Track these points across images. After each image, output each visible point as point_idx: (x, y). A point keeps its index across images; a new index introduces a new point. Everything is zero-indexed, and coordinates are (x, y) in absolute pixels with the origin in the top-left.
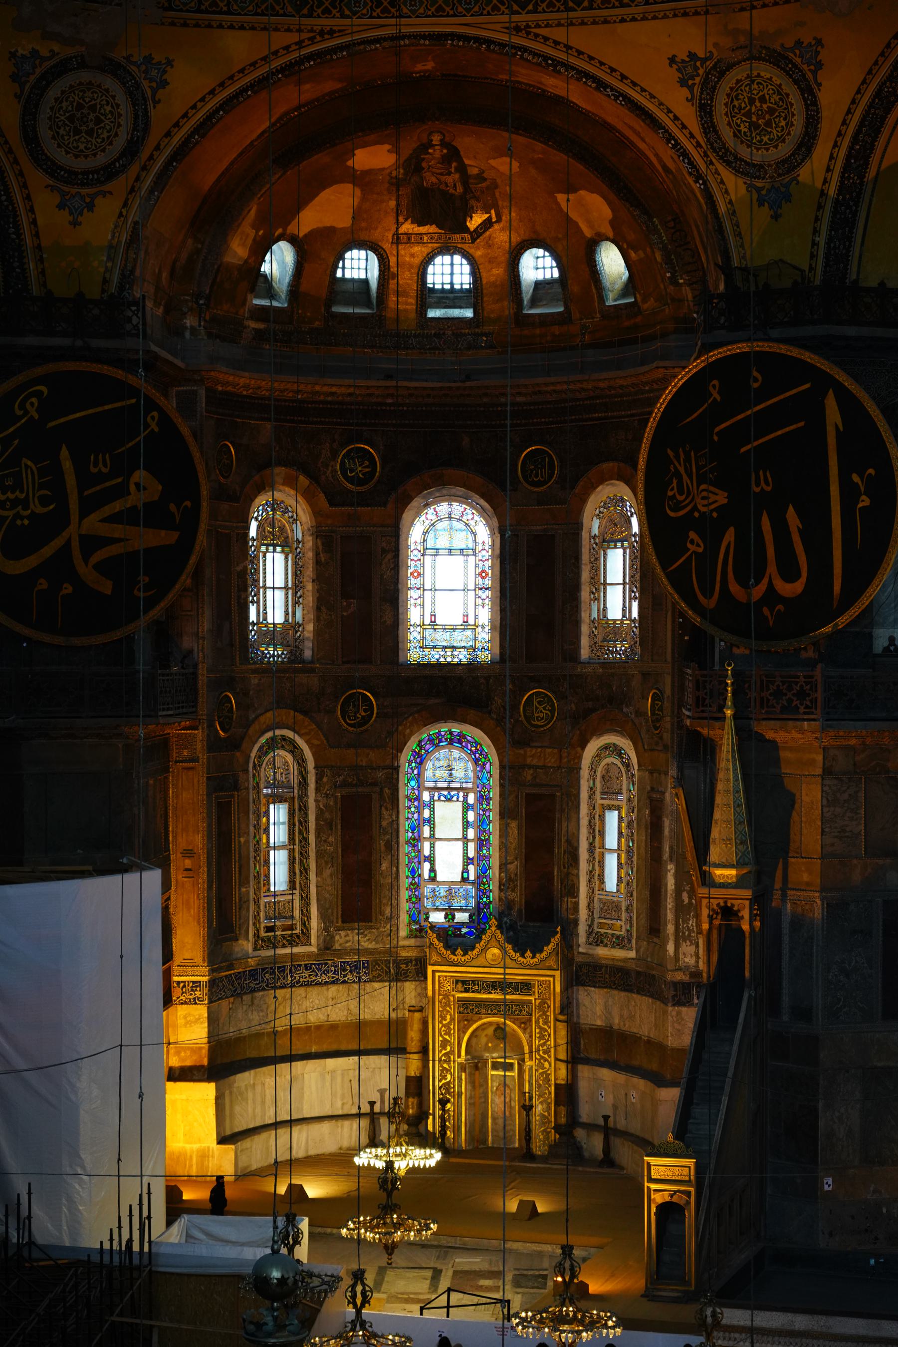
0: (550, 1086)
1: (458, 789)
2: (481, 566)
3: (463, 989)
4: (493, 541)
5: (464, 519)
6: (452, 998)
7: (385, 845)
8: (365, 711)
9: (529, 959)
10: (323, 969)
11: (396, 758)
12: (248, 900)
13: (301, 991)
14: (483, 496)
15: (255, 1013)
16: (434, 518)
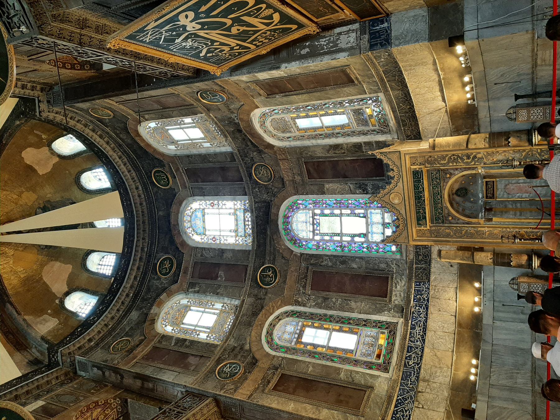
0: (498, 152)
1: (313, 219)
2: (209, 206)
3: (424, 220)
4: (199, 200)
5: (190, 214)
6: (434, 228)
7: (342, 264)
8: (269, 271)
9: (395, 174)
10: (416, 315)
11: (295, 255)
12: (351, 371)
13: (429, 334)
14: (180, 204)
15: (436, 380)
16: (191, 229)
